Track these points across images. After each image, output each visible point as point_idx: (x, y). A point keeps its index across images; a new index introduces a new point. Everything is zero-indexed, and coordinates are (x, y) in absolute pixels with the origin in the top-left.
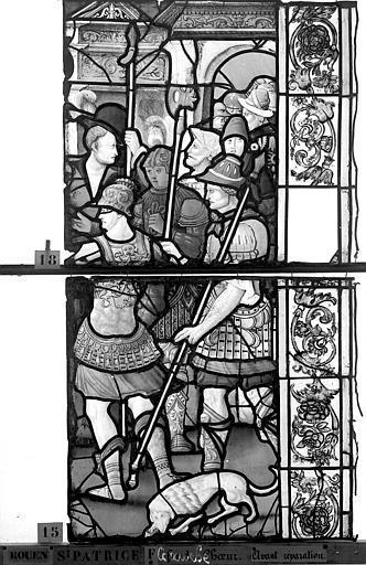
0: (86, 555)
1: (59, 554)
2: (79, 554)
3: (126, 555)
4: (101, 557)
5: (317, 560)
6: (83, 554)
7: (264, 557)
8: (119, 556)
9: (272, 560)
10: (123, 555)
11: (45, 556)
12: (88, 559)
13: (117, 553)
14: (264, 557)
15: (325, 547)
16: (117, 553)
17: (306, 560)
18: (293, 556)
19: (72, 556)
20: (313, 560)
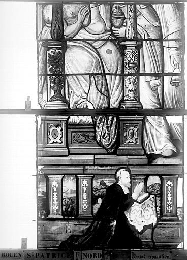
0: (42, 255)
2: (39, 254)
3: (64, 255)
8: (60, 255)
11: (21, 256)
12: (44, 258)
15: (171, 252)
18: (155, 257)
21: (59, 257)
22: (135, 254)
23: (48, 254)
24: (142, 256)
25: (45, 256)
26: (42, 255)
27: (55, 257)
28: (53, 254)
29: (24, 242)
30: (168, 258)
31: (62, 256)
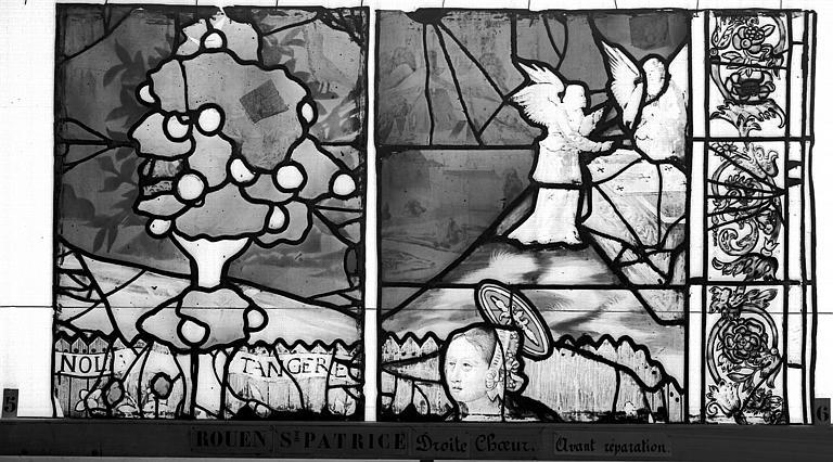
0: (324, 438)
1: (282, 436)
4: (348, 441)
5: (656, 454)
6: (319, 438)
7: (578, 447)
9: (584, 453)
10: (382, 437)
12: (328, 447)
13: (371, 436)
14: (578, 447)
16: (371, 436)
17: (643, 454)
19: (302, 437)
20: (650, 454)
21: (371, 447)
22: (565, 440)
23: (340, 435)
24: (587, 445)
25: (333, 442)
26: (324, 438)
27: (361, 446)
28: (355, 436)
29: (11, 397)
30: (662, 448)
31: (381, 445)
